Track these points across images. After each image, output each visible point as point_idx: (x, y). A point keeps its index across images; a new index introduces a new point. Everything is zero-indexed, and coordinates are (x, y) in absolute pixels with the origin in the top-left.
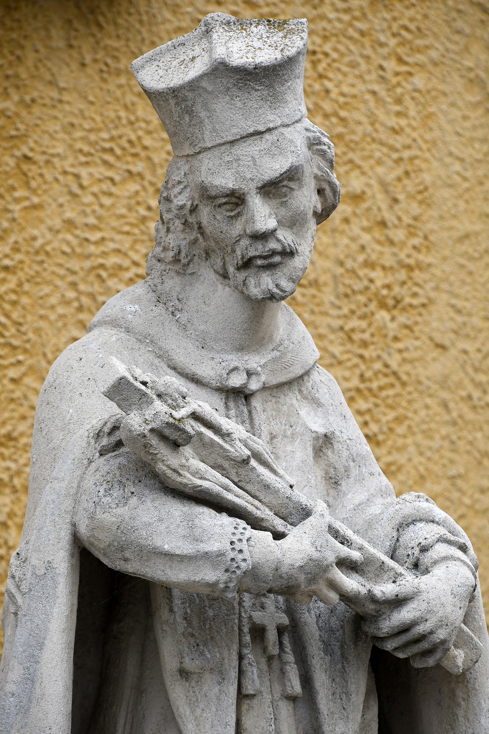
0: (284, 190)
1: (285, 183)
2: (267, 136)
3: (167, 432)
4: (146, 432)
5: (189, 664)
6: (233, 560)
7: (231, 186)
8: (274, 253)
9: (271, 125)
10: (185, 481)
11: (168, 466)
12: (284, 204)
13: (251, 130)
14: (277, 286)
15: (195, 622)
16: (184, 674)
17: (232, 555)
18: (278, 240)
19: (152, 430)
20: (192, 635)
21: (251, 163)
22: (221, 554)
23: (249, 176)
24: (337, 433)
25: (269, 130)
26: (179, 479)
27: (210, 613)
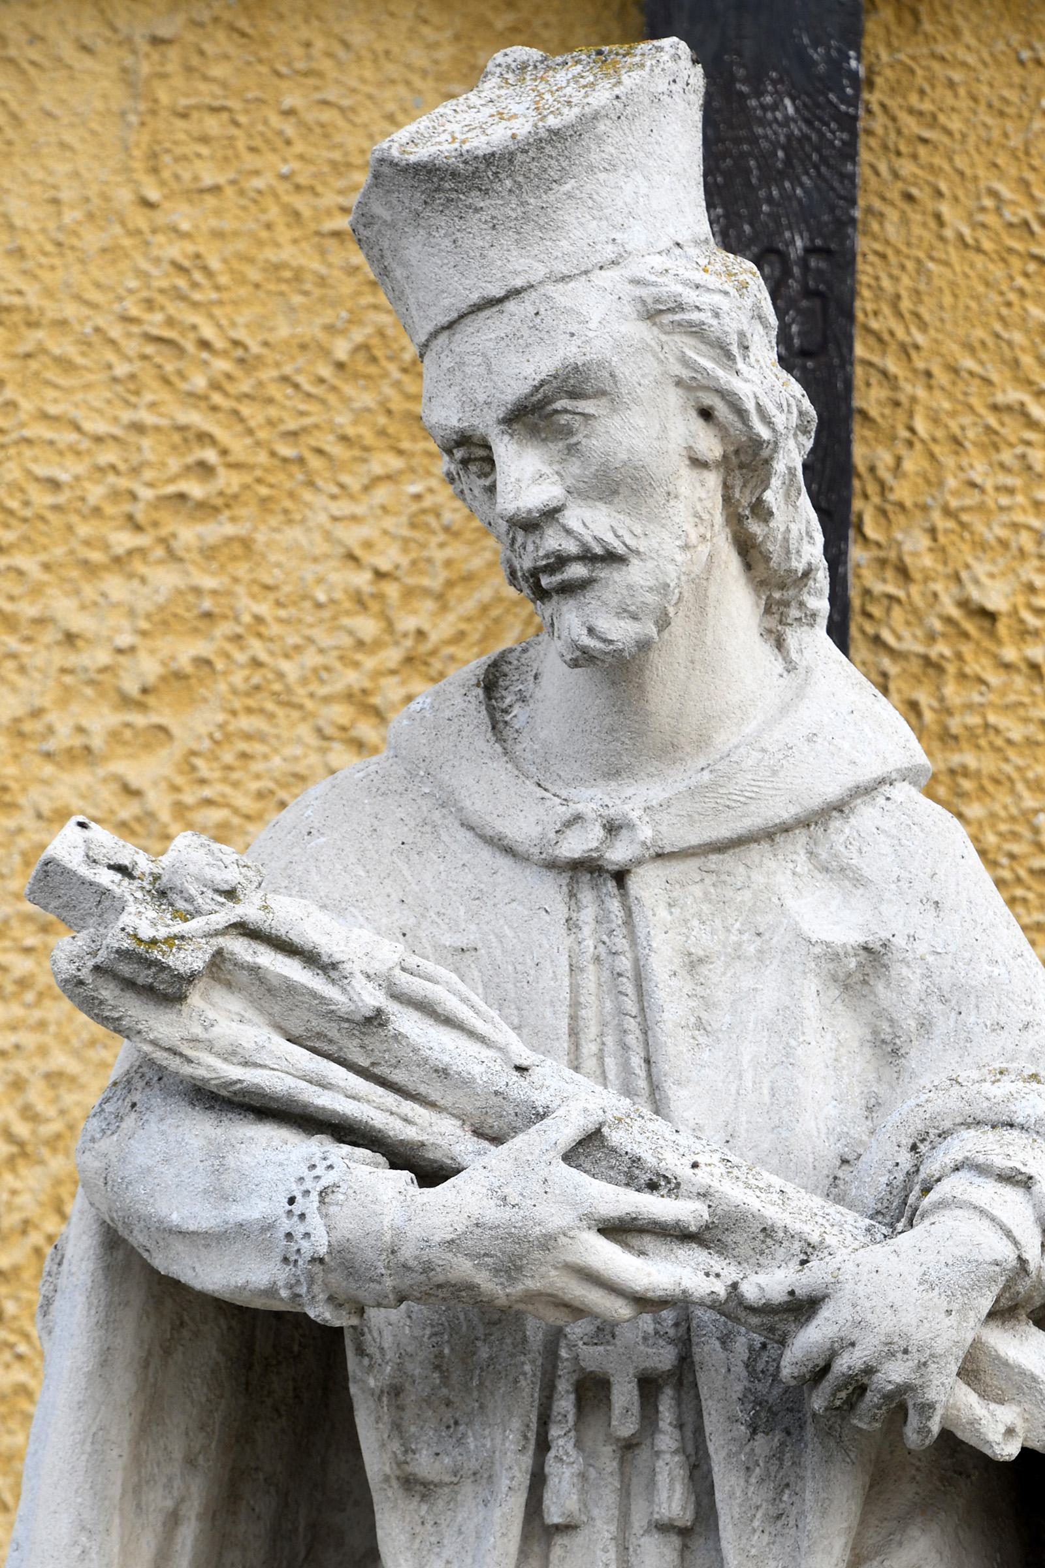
0: (564, 419)
1: (558, 405)
2: (511, 306)
3: (126, 969)
4: (85, 974)
5: (425, 1465)
6: (289, 1236)
7: (454, 422)
8: (561, 561)
9: (519, 282)
10: (201, 1072)
11: (154, 1043)
12: (572, 450)
13: (475, 297)
14: (591, 631)
15: (456, 1376)
16: (414, 1486)
17: (286, 1225)
18: (568, 532)
19: (97, 968)
20: (448, 1404)
21: (482, 370)
22: (268, 1227)
23: (481, 397)
24: (900, 942)
25: (515, 293)
26: (187, 1070)
27: (484, 1352)
